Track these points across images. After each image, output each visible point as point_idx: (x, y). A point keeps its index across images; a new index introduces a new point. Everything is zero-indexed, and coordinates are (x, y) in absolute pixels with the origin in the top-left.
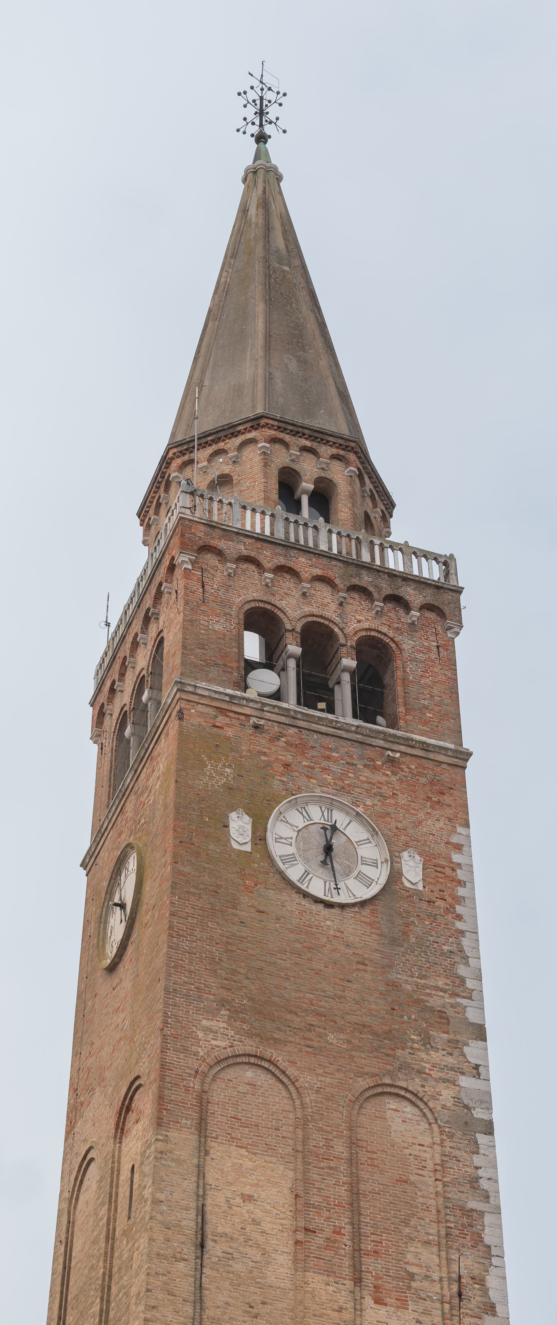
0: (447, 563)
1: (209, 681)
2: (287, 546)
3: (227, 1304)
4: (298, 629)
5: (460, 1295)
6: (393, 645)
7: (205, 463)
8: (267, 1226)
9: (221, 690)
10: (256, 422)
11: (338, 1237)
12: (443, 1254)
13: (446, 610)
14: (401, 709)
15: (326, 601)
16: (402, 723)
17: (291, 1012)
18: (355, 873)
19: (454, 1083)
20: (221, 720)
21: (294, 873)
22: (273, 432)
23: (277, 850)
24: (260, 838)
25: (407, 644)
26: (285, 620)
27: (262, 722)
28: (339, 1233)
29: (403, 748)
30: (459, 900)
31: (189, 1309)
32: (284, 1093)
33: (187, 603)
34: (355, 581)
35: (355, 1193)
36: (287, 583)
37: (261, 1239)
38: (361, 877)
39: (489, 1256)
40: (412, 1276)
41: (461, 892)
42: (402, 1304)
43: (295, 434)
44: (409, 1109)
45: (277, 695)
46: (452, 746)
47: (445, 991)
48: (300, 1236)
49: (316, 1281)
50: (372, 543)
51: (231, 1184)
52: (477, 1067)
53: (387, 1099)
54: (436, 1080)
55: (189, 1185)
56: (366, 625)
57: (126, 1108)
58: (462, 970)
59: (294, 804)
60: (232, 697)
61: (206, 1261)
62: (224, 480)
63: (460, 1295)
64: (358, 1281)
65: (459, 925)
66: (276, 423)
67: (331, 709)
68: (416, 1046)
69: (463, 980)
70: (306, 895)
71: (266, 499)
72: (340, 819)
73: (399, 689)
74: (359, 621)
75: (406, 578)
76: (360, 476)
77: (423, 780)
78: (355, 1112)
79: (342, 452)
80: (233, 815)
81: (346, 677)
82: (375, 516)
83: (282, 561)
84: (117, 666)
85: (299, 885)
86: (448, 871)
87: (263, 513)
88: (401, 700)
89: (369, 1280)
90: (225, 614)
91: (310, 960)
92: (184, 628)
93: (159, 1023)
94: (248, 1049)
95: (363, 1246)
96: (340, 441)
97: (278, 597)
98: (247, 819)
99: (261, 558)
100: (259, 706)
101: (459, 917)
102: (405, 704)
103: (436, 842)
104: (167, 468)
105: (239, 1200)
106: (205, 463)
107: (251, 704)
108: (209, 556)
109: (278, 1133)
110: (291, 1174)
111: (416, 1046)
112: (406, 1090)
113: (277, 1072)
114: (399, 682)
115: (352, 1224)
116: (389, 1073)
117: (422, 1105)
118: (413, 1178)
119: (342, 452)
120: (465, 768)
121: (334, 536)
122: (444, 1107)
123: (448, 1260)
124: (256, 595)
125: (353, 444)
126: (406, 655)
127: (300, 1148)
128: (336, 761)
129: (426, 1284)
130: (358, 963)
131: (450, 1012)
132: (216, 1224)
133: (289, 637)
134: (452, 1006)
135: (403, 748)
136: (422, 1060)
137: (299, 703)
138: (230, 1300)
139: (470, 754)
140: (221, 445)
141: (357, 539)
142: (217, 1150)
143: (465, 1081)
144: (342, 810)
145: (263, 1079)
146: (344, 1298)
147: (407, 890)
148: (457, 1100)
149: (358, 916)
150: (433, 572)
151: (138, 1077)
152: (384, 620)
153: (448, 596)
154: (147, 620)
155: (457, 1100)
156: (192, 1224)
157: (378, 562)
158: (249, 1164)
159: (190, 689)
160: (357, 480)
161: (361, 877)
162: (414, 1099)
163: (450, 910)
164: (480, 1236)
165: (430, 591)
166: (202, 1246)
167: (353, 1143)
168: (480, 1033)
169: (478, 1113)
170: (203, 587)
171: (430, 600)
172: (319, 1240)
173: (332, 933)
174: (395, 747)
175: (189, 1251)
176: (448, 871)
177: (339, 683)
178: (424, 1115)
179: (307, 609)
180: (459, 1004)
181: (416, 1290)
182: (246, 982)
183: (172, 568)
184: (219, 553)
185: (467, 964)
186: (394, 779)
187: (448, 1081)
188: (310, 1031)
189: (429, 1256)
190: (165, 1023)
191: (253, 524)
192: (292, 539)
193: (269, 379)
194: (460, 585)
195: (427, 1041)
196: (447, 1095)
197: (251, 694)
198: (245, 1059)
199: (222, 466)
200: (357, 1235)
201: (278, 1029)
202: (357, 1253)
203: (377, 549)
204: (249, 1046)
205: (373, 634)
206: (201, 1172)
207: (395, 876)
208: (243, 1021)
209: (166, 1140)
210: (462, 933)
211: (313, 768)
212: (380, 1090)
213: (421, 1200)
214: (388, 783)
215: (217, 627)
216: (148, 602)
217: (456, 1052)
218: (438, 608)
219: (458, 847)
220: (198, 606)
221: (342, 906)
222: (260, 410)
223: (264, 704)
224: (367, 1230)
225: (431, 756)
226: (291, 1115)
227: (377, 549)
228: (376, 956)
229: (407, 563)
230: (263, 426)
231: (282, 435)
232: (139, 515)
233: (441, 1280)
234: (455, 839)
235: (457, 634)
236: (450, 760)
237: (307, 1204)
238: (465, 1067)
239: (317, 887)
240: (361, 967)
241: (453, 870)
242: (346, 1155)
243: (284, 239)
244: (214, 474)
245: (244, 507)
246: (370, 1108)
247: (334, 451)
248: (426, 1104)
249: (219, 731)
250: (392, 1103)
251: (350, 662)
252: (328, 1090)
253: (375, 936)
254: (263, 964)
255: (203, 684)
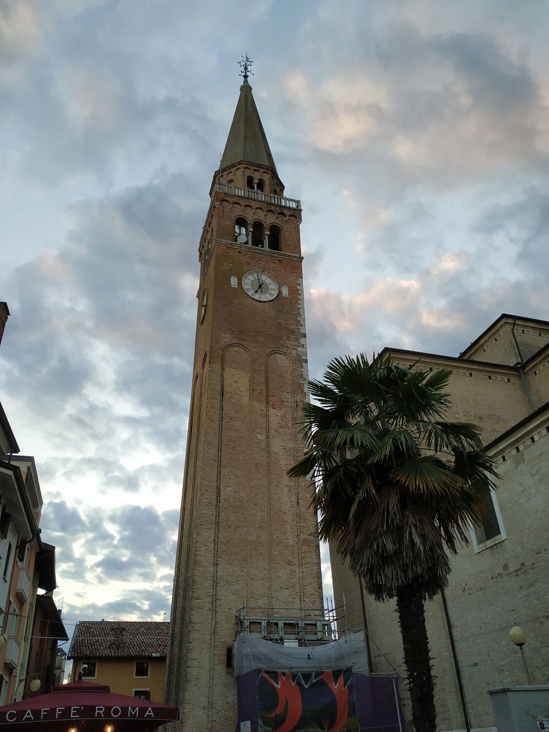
0: (298, 202)
1: (225, 239)
2: (248, 199)
3: (230, 410)
4: (252, 224)
5: (297, 406)
6: (281, 227)
7: (226, 176)
8: (242, 390)
9: (228, 242)
10: (240, 163)
11: (262, 392)
12: (292, 395)
13: (297, 216)
14: (283, 246)
15: (260, 215)
16: (283, 250)
17: (249, 332)
18: (268, 293)
19: (296, 349)
20: (228, 250)
21: (250, 293)
22: (245, 165)
23: (245, 287)
24: (240, 284)
25: (285, 227)
26: (248, 221)
27: (240, 251)
28: (262, 391)
29: (283, 257)
30: (299, 299)
31: (219, 412)
32: (247, 354)
33: (218, 217)
34: (269, 209)
35: (267, 380)
36: (249, 209)
37: (240, 393)
38: (270, 294)
39: (305, 395)
40: (283, 401)
41: (300, 297)
42: (280, 408)
43: (252, 166)
44: (283, 357)
45: (246, 243)
46: (298, 256)
47: (294, 325)
48: (251, 392)
49: (255, 403)
50: (275, 197)
51: (231, 378)
52: (303, 345)
53: (277, 354)
54: (291, 349)
55: (219, 379)
56: (273, 222)
57: (204, 360)
58: (299, 319)
59: (250, 274)
60: (231, 243)
61: (224, 399)
62: (231, 181)
63: (297, 406)
64: (267, 403)
65: (299, 306)
66: (246, 163)
67: (262, 247)
68: (285, 340)
69: (299, 321)
70: (253, 299)
71: (243, 186)
72: (264, 278)
73: (283, 240)
74: (271, 220)
75: (285, 207)
76: (273, 178)
77: (289, 266)
78: (267, 358)
79: (267, 171)
80: (232, 277)
81: (267, 237)
82: (278, 190)
83: (247, 203)
84: (204, 239)
85: (252, 296)
86: (296, 291)
87: (241, 189)
88: (283, 243)
89: (271, 403)
90: (230, 220)
91: (255, 317)
92: (217, 224)
93: (210, 336)
94: (236, 342)
95: (269, 394)
96: (266, 167)
97: (246, 214)
98: (236, 279)
99: (240, 203)
100: (240, 246)
101: (299, 304)
102: (284, 244)
103: (293, 283)
104: (215, 179)
105: (233, 383)
106: (226, 176)
107: (238, 246)
108: (225, 202)
109: (245, 364)
110: (249, 375)
111: (285, 340)
112: (282, 352)
113: (245, 348)
114: (283, 238)
115: (266, 388)
116: (278, 348)
117: (287, 356)
118: (284, 375)
119: (267, 171)
120: (302, 262)
121: (263, 195)
122: (293, 356)
123: (294, 397)
124: (239, 214)
125: (270, 168)
126: (285, 230)
127: (251, 368)
128: (263, 261)
129: (287, 403)
130: (269, 317)
131: (296, 330)
132: (227, 389)
133: (249, 226)
134: (296, 328)
135: (283, 257)
136: (287, 344)
137: (252, 245)
138: (231, 409)
139: (303, 258)
140: (230, 170)
141: (270, 196)
142: (227, 369)
143: (299, 349)
144: (264, 275)
145: (240, 350)
146: (263, 407)
147: (283, 297)
148: (297, 354)
149: (269, 305)
150: (294, 205)
151: (206, 352)
152: (278, 220)
153: (298, 212)
154: (210, 224)
155: (297, 354)
156: (220, 389)
157: (279, 204)
158: (236, 373)
159: (219, 242)
160: (272, 179)
161: (270, 294)
162: (285, 354)
163: (296, 302)
164: (303, 390)
165: (292, 211)
166: (223, 395)
167: (267, 366)
168: (304, 336)
169: (303, 357)
170: (223, 212)
171: (292, 213)
172: (256, 392)
173: (261, 309)
174: (281, 257)
175: (219, 397)
176: (296, 291)
177: (265, 239)
178: (288, 358)
179: (255, 218)
180: (298, 328)
181: (284, 405)
182: (236, 324)
183: (215, 207)
184: (228, 201)
185: (301, 317)
186: (280, 265)
187: (295, 349)
188: (254, 336)
189: (289, 396)
190: (212, 336)
191: (238, 193)
192: (250, 197)
193: (245, 150)
194: (301, 209)
195: (289, 339)
196: (294, 353)
197: (237, 243)
198: (235, 345)
199: (230, 177)
200: (267, 391)
201: (245, 336)
202: (267, 395)
203: (276, 199)
204: (236, 341)
205: (275, 224)
206: (222, 376)
207: (280, 293)
208: (235, 334)
209: (212, 367)
210: (300, 308)
211: (256, 263)
212: (275, 352)
213: (286, 381)
214: (278, 267)
215: (227, 223)
216: (210, 218)
217: (297, 341)
218: (294, 216)
219: (299, 285)
220: (222, 217)
221: (264, 302)
222: (242, 159)
223: (241, 245)
224: (270, 389)
225: (292, 259)
226: (249, 360)
227: (276, 199)
228: (274, 316)
229: (286, 203)
230: (242, 164)
231: (248, 166)
232: (210, 194)
233: (291, 402)
234: (298, 282)
235: (300, 223)
236: (298, 260)
237: (253, 383)
238: (300, 345)
239: (257, 297)
240: (269, 319)
241: (297, 291)
242: (264, 369)
243: (252, 107)
244: (229, 179)
245: (235, 188)
246: (271, 357)
247: (264, 170)
248: (288, 355)
249: (228, 253)
250: (278, 355)
251: (268, 233)
252: (259, 352)
253: (274, 310)
254: (241, 319)
255: (223, 240)
